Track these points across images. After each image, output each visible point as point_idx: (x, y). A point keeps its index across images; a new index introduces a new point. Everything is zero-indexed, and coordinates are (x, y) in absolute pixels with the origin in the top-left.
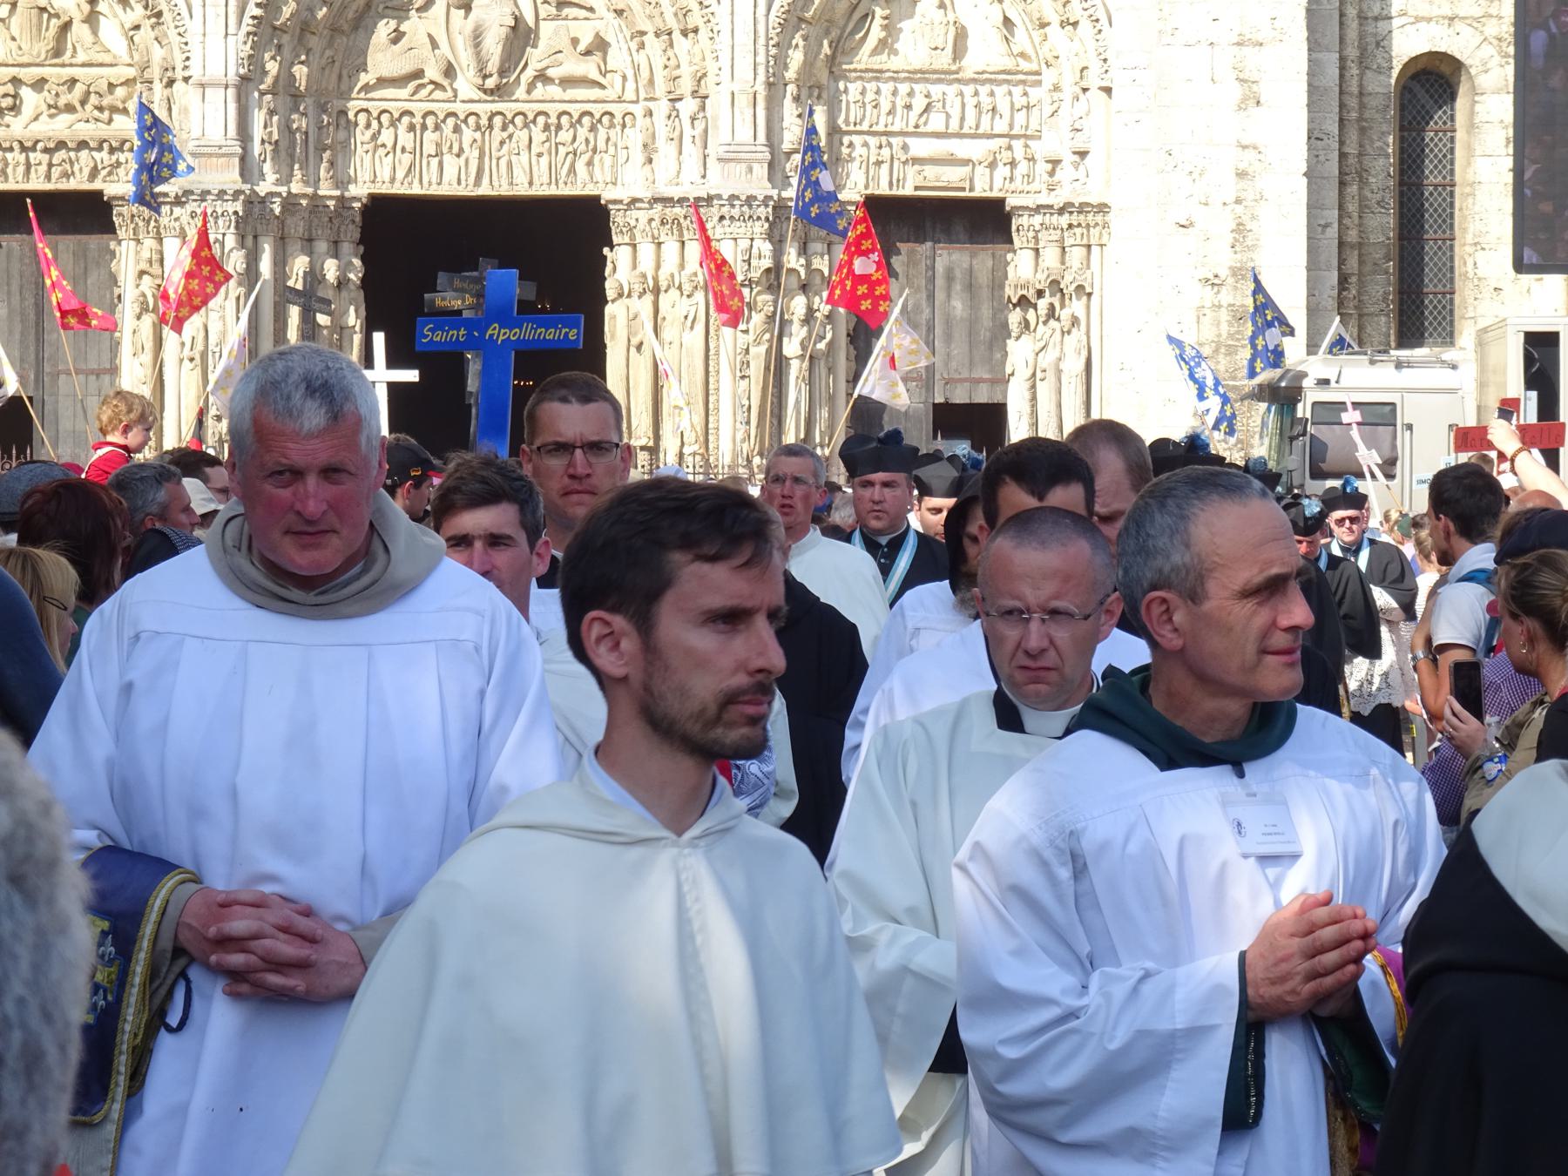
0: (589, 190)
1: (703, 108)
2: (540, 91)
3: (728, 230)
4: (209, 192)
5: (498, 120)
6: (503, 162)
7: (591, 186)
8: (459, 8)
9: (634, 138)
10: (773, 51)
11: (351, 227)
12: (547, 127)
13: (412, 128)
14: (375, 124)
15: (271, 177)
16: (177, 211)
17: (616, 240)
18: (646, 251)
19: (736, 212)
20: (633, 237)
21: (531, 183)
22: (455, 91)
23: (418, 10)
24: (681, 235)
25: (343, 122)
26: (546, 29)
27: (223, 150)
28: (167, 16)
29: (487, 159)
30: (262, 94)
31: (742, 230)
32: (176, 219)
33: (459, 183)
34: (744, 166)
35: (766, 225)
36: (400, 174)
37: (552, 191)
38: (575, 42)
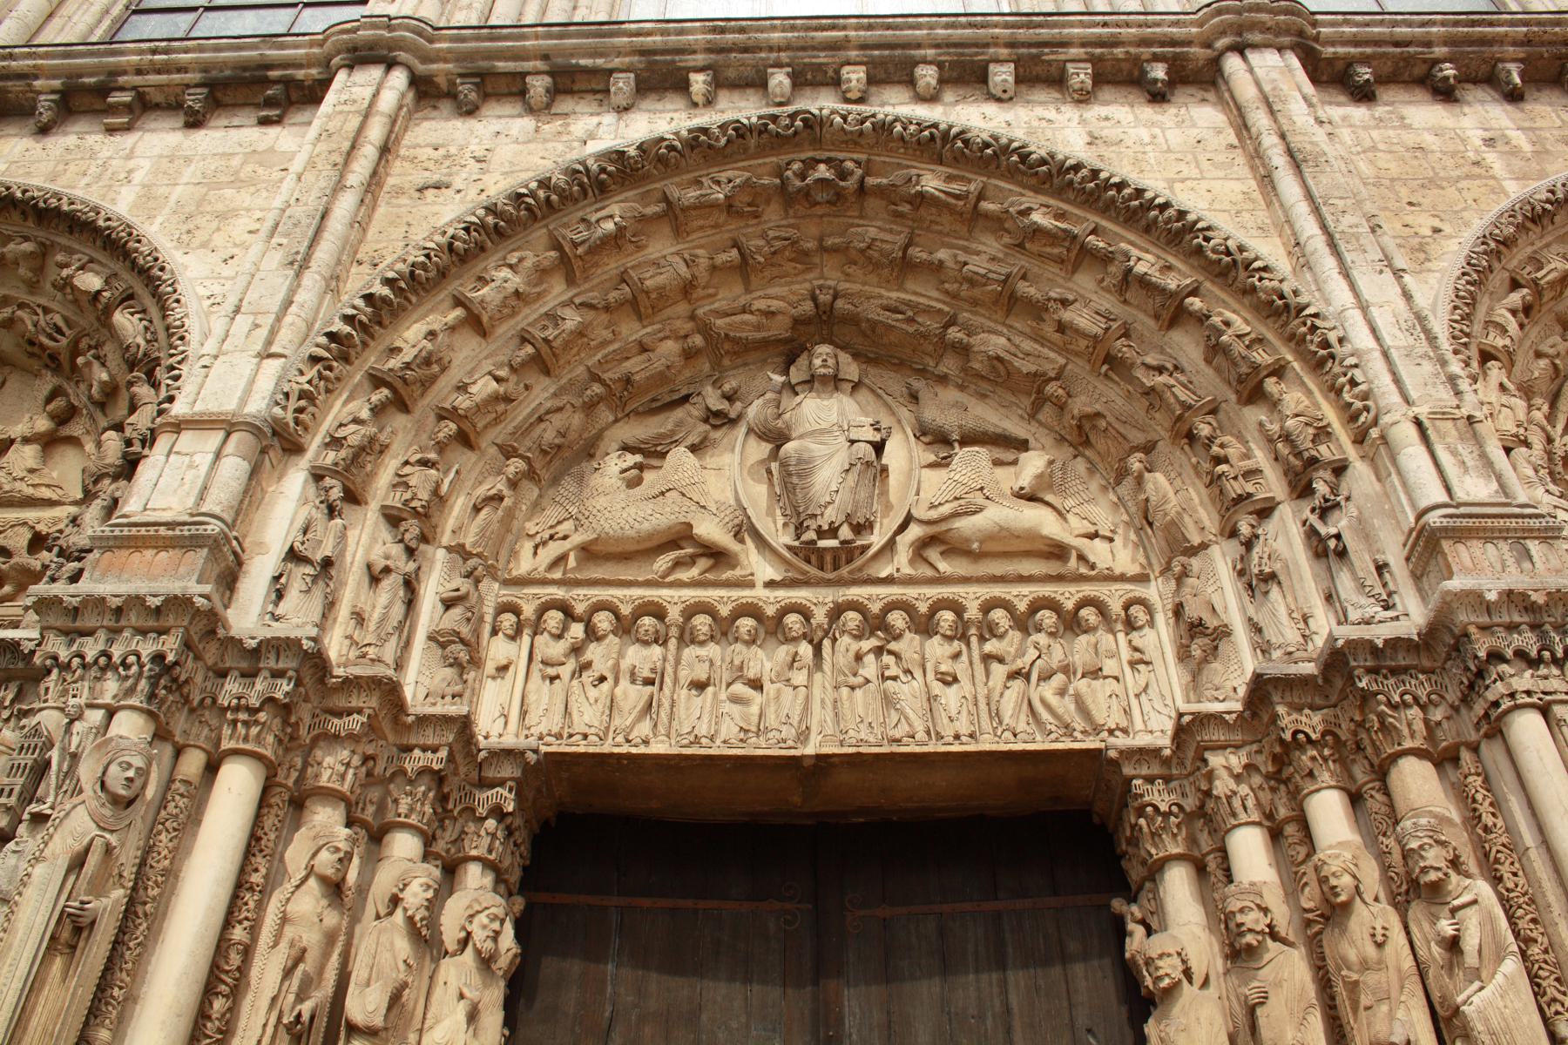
9: (1160, 638)
11: (491, 824)
14: (577, 630)
18: (1250, 851)
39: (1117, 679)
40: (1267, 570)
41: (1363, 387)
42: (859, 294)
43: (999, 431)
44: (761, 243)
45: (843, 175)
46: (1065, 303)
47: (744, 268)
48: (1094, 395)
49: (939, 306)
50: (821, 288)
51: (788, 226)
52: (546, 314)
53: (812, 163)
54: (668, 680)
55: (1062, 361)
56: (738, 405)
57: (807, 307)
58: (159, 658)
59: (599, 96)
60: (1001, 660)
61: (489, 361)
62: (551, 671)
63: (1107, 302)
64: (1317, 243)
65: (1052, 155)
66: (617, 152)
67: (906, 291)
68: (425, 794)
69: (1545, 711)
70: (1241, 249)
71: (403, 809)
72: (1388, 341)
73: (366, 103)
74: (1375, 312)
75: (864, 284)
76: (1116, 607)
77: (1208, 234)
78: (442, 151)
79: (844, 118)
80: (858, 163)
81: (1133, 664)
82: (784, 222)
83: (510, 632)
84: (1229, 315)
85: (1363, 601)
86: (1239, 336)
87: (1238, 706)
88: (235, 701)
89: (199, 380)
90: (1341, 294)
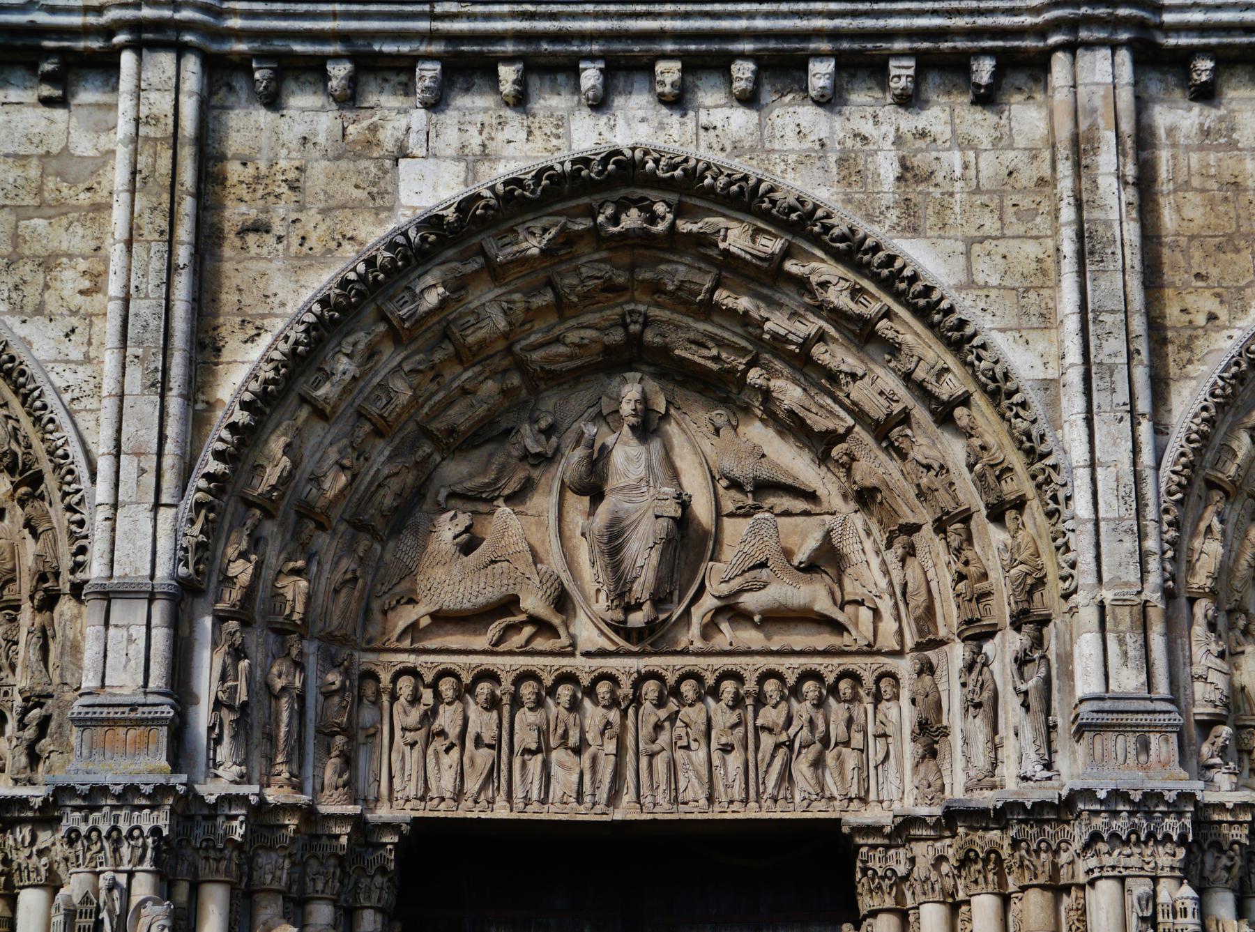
0: (819, 811)
1: (1038, 642)
2: (728, 635)
3: (1108, 861)
4: (103, 790)
5: (650, 688)
6: (660, 763)
7: (821, 805)
8: (580, 492)
10: (1172, 534)
11: (379, 880)
12: (738, 702)
13: (493, 703)
14: (427, 696)
15: (229, 771)
16: (44, 838)
17: (866, 903)
19: (1121, 825)
20: (900, 897)
21: (710, 799)
22: (573, 638)
23: (508, 500)
24: (1002, 883)
25: (369, 689)
26: (735, 530)
27: (139, 714)
28: (50, 482)
29: (630, 757)
30: (220, 619)
31: (1134, 861)
32: (41, 853)
33: (580, 798)
34: (1132, 738)
35: (1181, 853)
36: (472, 785)
37: (752, 812)
38: (788, 554)
39: (862, 751)
40: (977, 700)
41: (1071, 556)
42: (668, 322)
43: (790, 481)
44: (574, 281)
45: (653, 218)
46: (854, 377)
47: (561, 307)
48: (873, 465)
49: (744, 343)
50: (631, 312)
51: (601, 261)
52: (379, 384)
53: (623, 206)
54: (505, 747)
55: (851, 422)
56: (554, 439)
57: (617, 336)
58: (156, 831)
59: (403, 78)
60: (770, 730)
61: (335, 448)
62: (410, 736)
63: (891, 382)
64: (1074, 377)
65: (852, 231)
66: (436, 216)
67: (713, 323)
68: (334, 874)
69: (1122, 880)
70: (1006, 376)
71: (320, 886)
72: (1102, 514)
73: (170, 120)
74: (1099, 470)
75: (673, 311)
76: (868, 679)
77: (983, 353)
78: (251, 170)
79: (657, 161)
80: (669, 206)
81: (876, 736)
82: (596, 256)
83: (373, 699)
84: (990, 439)
85: (1033, 756)
86: (992, 466)
87: (938, 811)
88: (204, 844)
89: (107, 535)
90: (1079, 453)
